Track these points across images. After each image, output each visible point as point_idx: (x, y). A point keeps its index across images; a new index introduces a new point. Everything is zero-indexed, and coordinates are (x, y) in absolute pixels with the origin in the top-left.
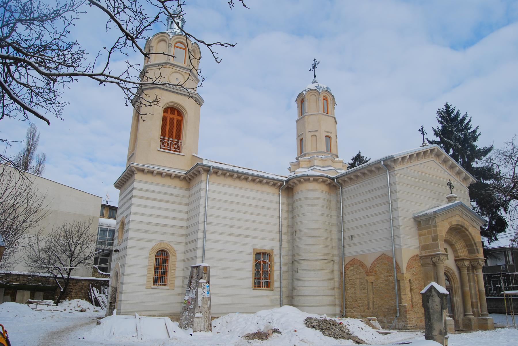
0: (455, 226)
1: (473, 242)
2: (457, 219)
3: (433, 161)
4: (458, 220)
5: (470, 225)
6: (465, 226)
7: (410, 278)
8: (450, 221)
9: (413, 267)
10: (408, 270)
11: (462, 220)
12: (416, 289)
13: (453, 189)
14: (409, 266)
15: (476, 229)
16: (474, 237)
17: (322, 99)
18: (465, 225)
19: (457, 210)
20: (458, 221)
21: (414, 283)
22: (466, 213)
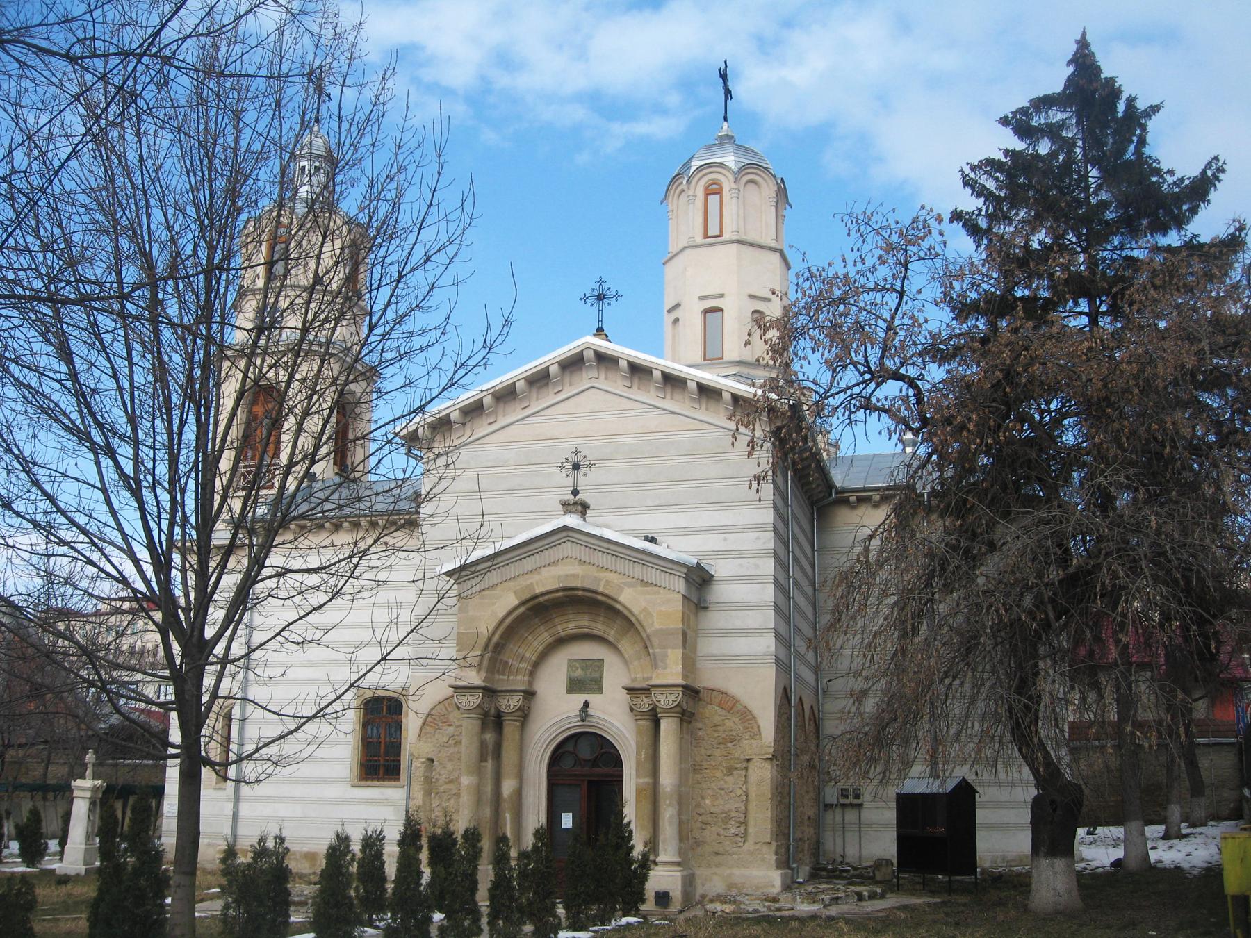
0: (560, 594)
1: (644, 636)
2: (561, 573)
3: (593, 390)
4: (567, 576)
5: (629, 580)
6: (601, 589)
7: (430, 756)
8: (528, 582)
9: (451, 725)
10: (426, 734)
11: (592, 571)
12: (446, 783)
13: (585, 475)
14: (432, 720)
15: (661, 590)
16: (641, 617)
17: (700, 193)
18: (602, 583)
19: (569, 543)
20: (575, 576)
21: (445, 768)
22: (605, 545)
